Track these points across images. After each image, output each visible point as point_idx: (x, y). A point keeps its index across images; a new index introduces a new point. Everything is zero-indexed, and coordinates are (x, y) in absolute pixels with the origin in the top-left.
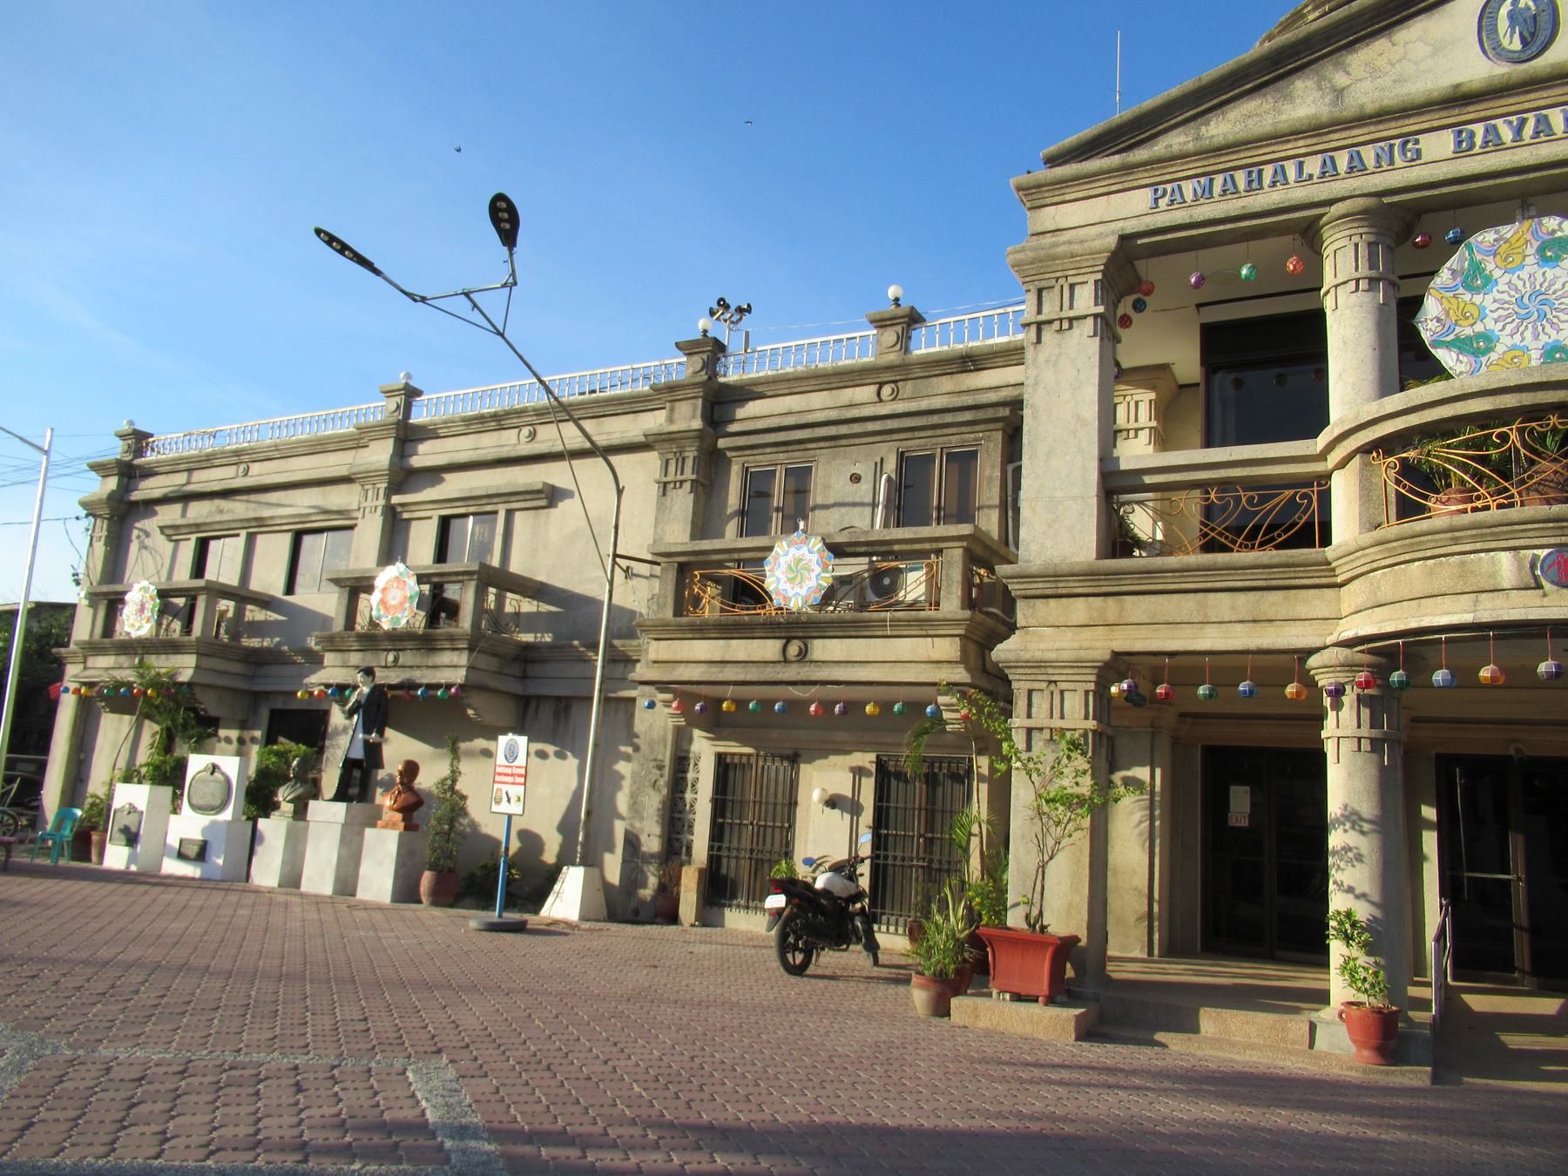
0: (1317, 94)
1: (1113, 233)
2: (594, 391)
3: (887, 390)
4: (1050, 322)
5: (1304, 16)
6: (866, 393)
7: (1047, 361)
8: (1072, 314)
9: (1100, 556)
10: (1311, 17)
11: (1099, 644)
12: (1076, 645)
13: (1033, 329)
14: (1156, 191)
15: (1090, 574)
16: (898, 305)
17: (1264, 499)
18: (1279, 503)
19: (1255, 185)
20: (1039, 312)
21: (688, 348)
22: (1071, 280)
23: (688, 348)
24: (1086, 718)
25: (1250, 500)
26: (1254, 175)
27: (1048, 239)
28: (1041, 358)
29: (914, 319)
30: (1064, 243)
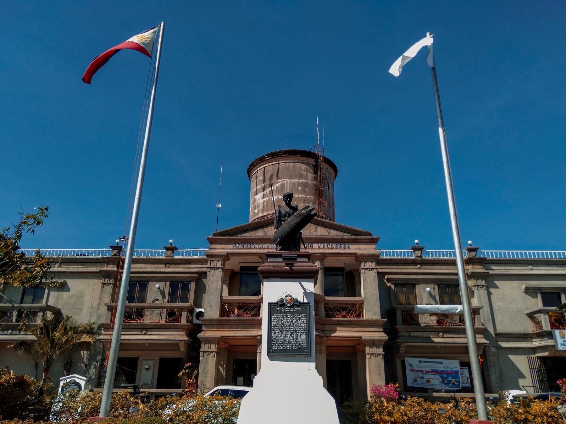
0: (262, 232)
1: (226, 252)
2: (81, 255)
3: (168, 265)
4: (213, 268)
5: (266, 158)
6: (163, 266)
7: (211, 275)
8: (217, 267)
9: (220, 317)
10: (267, 159)
11: (219, 334)
12: (214, 334)
13: (209, 269)
14: (234, 245)
15: (218, 320)
16: (171, 245)
17: (249, 306)
18: (251, 308)
19: (251, 247)
20: (210, 265)
21: (113, 248)
22: (217, 260)
23: (113, 248)
24: (215, 349)
25: (247, 306)
26: (251, 245)
27: (213, 251)
28: (210, 275)
29: (175, 248)
30: (216, 252)
